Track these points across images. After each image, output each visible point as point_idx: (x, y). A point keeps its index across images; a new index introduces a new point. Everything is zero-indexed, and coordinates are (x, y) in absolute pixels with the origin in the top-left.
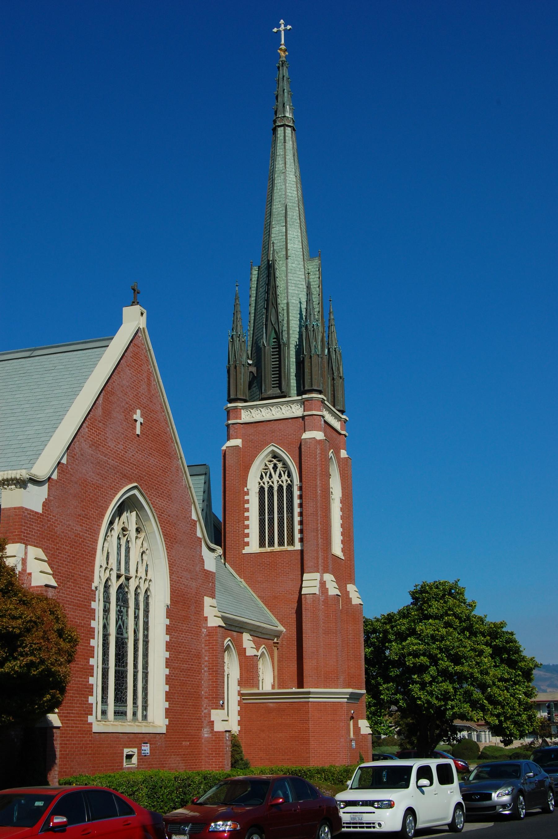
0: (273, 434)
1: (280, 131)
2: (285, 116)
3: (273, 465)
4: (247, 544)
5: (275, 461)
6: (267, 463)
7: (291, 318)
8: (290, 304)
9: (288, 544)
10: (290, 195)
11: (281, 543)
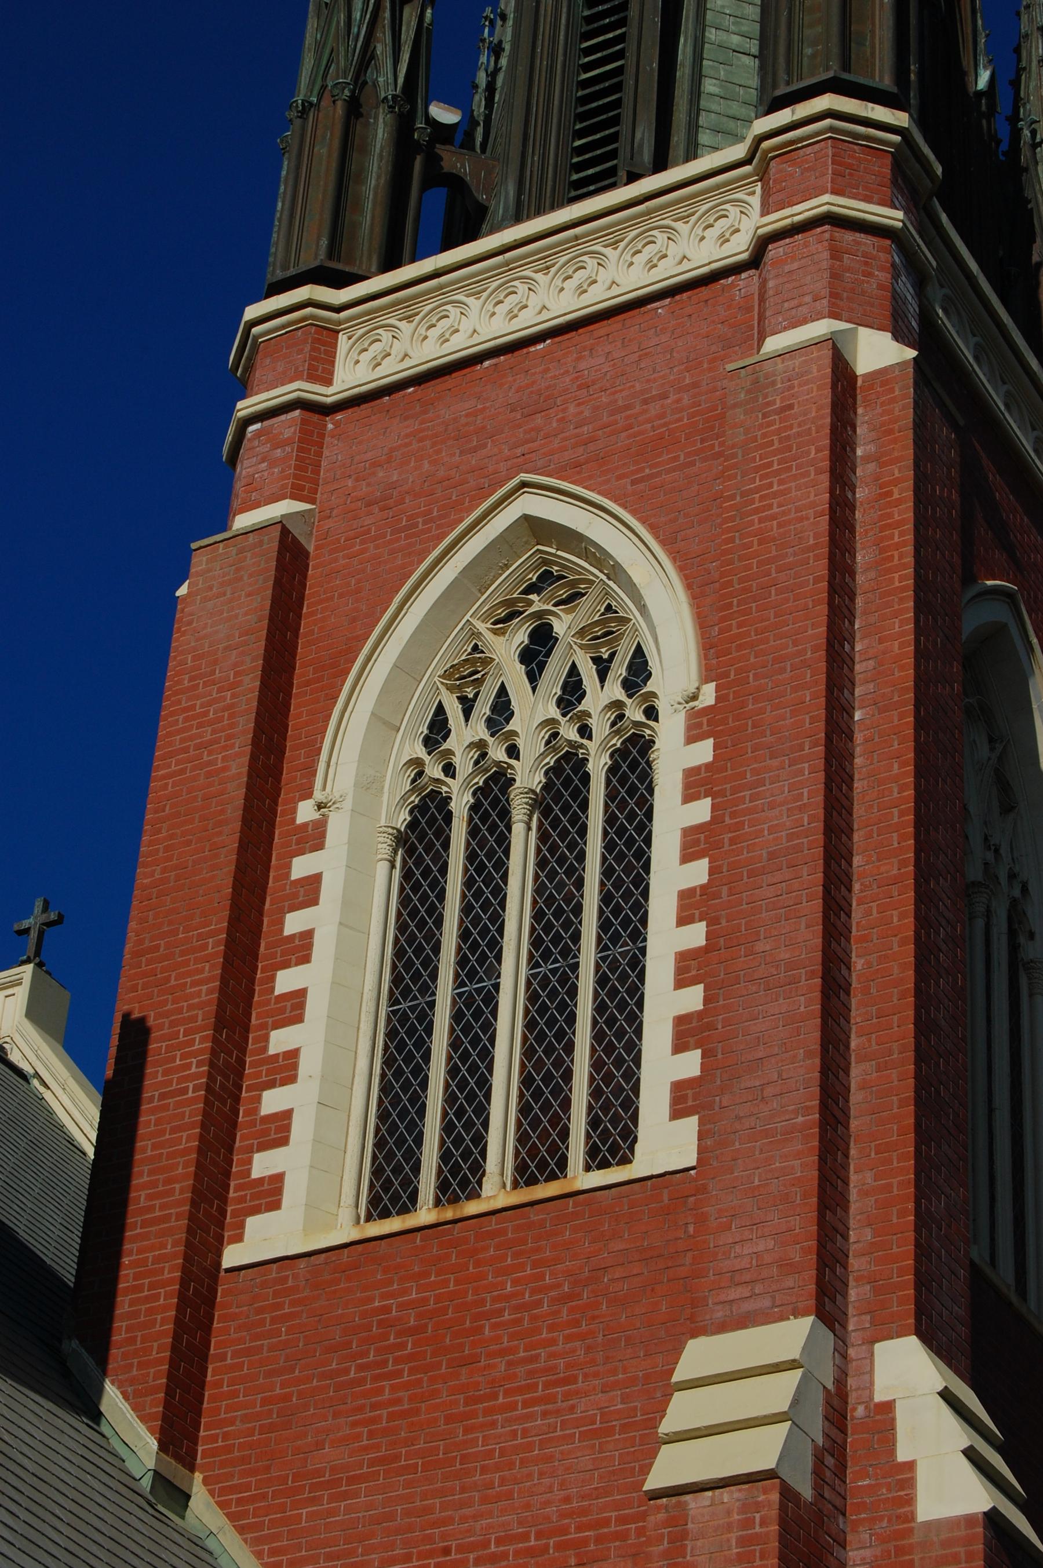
0: (539, 420)
3: (521, 636)
4: (269, 1194)
5: (537, 603)
6: (482, 627)
9: (596, 1160)
11: (539, 1159)
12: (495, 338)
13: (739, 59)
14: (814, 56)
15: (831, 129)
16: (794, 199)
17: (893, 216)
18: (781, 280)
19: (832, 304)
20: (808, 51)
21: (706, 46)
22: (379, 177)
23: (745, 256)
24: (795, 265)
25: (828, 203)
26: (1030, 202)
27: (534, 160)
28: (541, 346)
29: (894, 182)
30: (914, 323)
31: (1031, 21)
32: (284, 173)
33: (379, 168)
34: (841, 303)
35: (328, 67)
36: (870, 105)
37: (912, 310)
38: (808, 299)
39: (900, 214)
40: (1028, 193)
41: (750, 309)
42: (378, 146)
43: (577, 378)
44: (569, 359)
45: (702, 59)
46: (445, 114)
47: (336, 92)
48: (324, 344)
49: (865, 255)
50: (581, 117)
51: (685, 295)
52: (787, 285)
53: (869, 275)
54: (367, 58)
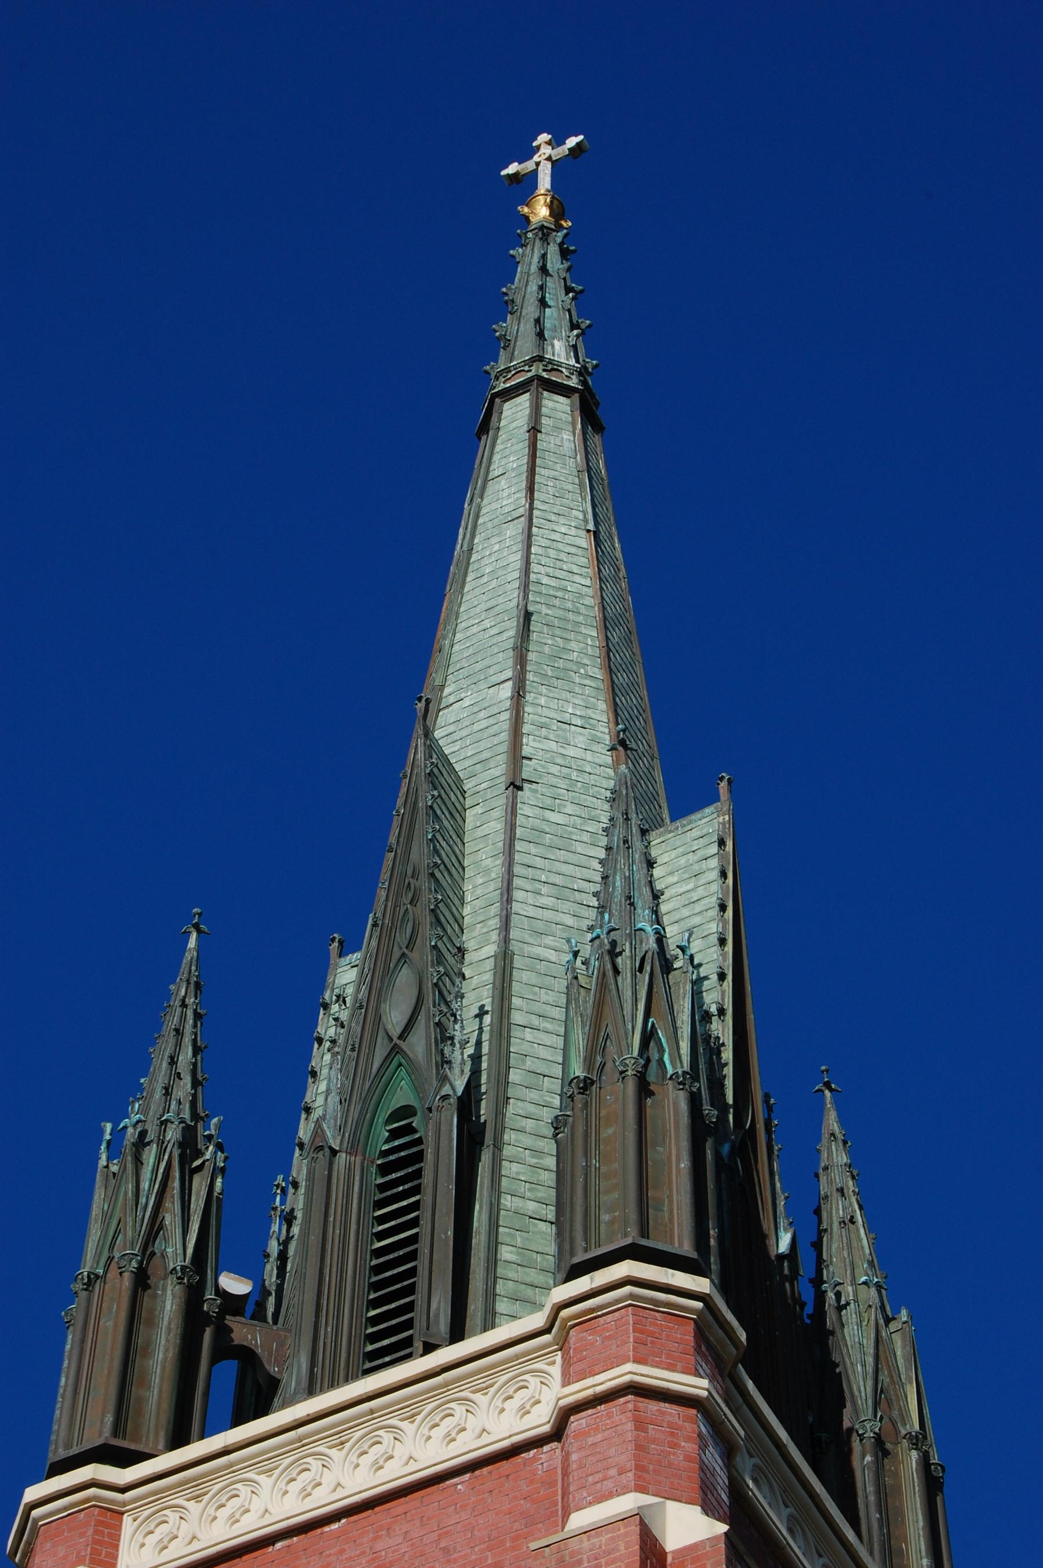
1: (514, 414)
2: (540, 358)
7: (517, 1017)
8: (518, 962)
10: (545, 580)
12: (288, 1518)
13: (535, 1225)
14: (611, 1223)
15: (631, 1296)
16: (596, 1369)
17: (698, 1385)
18: (584, 1453)
19: (637, 1478)
20: (605, 1217)
21: (502, 1212)
22: (167, 1350)
23: (546, 1428)
24: (599, 1437)
25: (630, 1373)
26: (837, 1365)
27: (326, 1331)
28: (335, 1526)
29: (698, 1350)
30: (724, 1496)
31: (830, 1182)
32: (68, 1347)
33: (168, 1341)
34: (646, 1475)
35: (115, 1238)
36: (670, 1271)
37: (721, 1482)
38: (613, 1472)
39: (705, 1383)
40: (836, 1357)
41: (553, 1484)
42: (166, 1319)
43: (373, 1559)
44: (365, 1539)
45: (498, 1226)
46: (235, 1285)
47: (123, 1263)
48: (108, 1526)
49: (670, 1425)
50: (375, 1286)
51: (485, 1470)
52: (591, 1458)
53: (674, 1445)
54: (155, 1229)
